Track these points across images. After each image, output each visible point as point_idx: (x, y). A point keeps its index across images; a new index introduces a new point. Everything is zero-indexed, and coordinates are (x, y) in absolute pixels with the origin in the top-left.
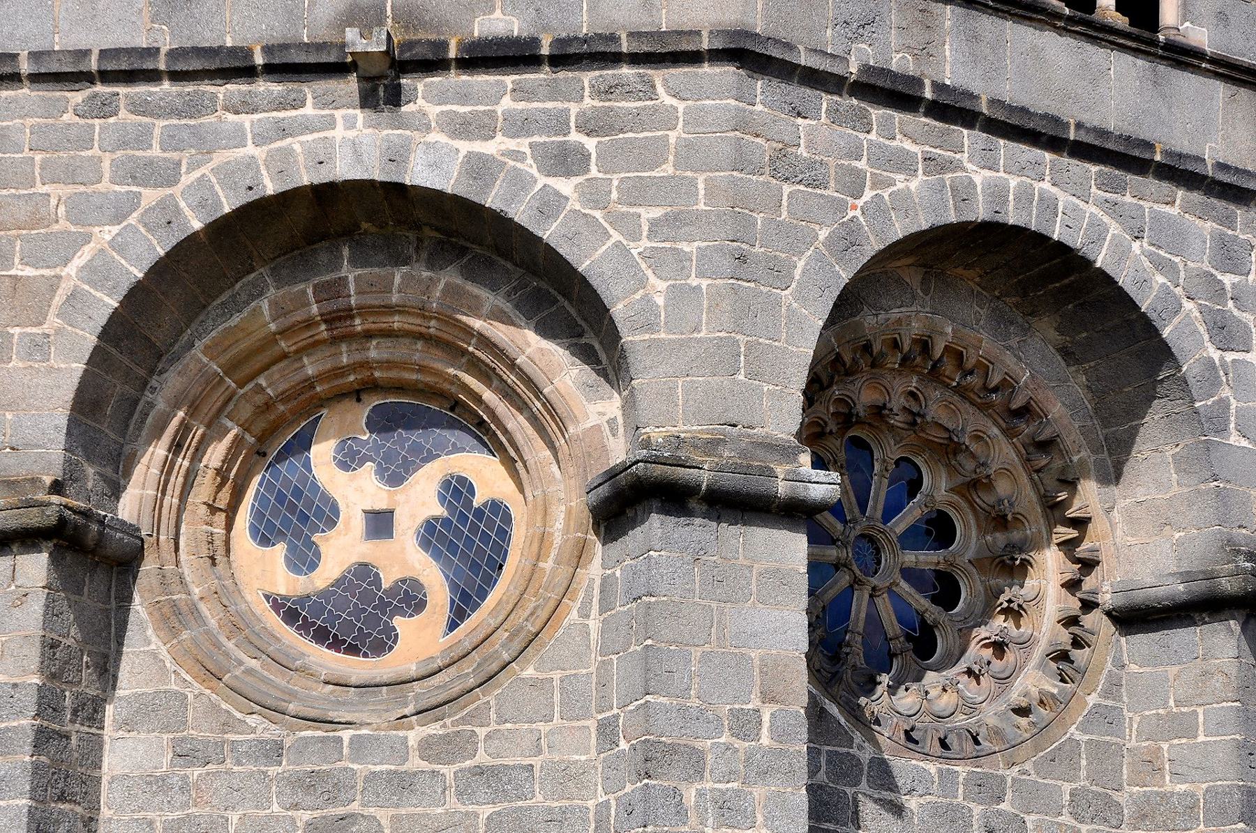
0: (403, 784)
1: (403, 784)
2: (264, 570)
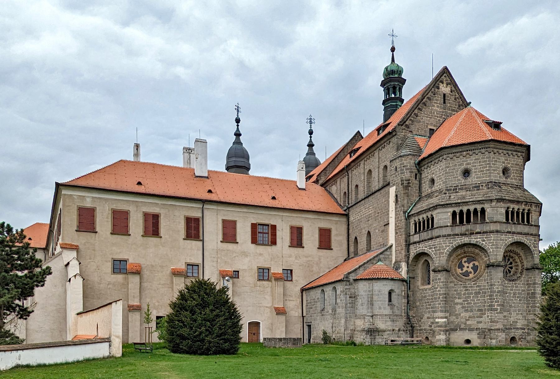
0: (472, 287)
1: (472, 287)
2: (459, 271)
